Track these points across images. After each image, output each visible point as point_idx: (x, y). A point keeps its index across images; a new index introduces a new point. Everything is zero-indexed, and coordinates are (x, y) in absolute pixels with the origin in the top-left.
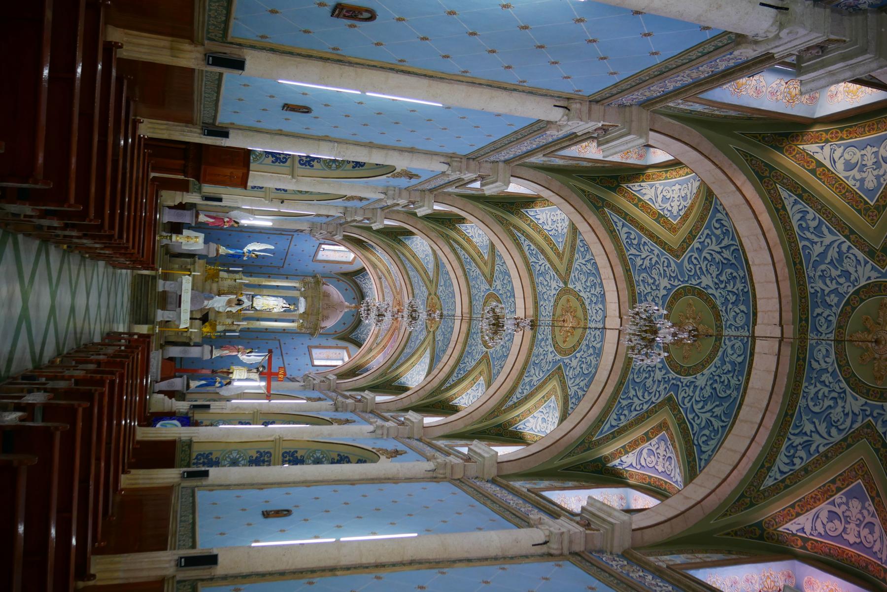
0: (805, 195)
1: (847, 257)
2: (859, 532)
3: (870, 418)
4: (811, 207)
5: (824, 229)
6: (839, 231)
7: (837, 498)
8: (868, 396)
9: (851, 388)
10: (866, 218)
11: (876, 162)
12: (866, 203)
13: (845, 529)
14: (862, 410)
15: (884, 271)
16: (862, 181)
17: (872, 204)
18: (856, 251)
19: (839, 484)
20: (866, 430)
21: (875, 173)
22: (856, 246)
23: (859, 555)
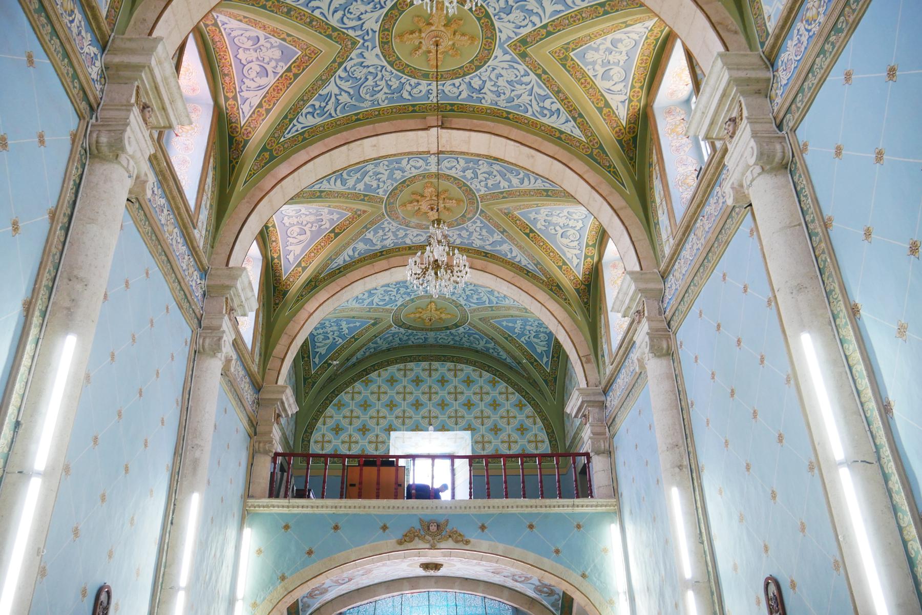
0: (601, 10)
1: (526, 18)
2: (252, 61)
3: (362, 41)
4: (587, 7)
5: (559, 7)
6: (553, 21)
7: (275, 41)
8: (383, 31)
9: (386, 15)
10: (559, 48)
11: (609, 63)
12: (573, 50)
13: (249, 49)
14: (368, 30)
15: (505, 46)
16: (597, 50)
17: (571, 54)
18: (530, 29)
19: (289, 39)
20: (349, 43)
21: (599, 61)
22: (534, 31)
23: (231, 65)
